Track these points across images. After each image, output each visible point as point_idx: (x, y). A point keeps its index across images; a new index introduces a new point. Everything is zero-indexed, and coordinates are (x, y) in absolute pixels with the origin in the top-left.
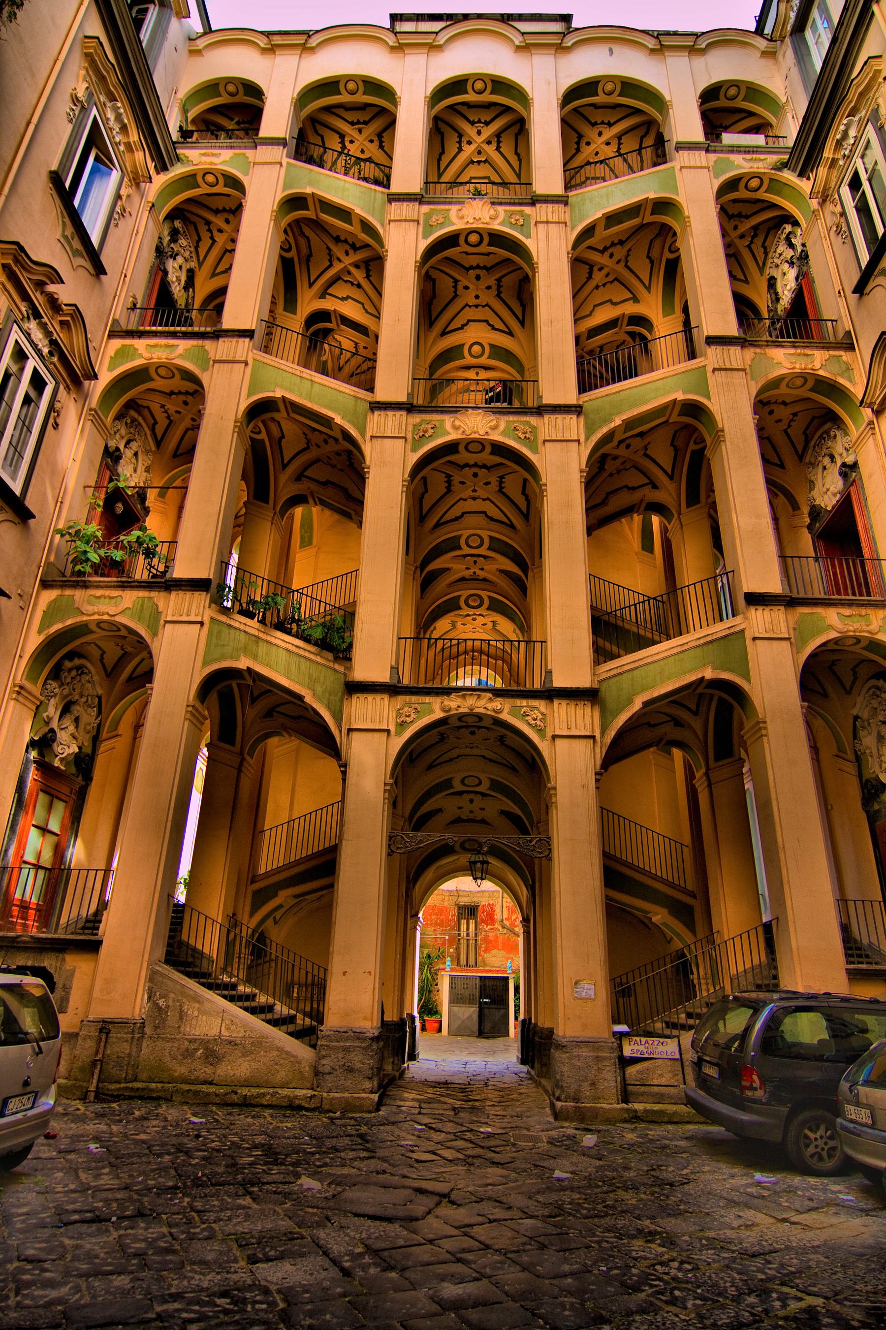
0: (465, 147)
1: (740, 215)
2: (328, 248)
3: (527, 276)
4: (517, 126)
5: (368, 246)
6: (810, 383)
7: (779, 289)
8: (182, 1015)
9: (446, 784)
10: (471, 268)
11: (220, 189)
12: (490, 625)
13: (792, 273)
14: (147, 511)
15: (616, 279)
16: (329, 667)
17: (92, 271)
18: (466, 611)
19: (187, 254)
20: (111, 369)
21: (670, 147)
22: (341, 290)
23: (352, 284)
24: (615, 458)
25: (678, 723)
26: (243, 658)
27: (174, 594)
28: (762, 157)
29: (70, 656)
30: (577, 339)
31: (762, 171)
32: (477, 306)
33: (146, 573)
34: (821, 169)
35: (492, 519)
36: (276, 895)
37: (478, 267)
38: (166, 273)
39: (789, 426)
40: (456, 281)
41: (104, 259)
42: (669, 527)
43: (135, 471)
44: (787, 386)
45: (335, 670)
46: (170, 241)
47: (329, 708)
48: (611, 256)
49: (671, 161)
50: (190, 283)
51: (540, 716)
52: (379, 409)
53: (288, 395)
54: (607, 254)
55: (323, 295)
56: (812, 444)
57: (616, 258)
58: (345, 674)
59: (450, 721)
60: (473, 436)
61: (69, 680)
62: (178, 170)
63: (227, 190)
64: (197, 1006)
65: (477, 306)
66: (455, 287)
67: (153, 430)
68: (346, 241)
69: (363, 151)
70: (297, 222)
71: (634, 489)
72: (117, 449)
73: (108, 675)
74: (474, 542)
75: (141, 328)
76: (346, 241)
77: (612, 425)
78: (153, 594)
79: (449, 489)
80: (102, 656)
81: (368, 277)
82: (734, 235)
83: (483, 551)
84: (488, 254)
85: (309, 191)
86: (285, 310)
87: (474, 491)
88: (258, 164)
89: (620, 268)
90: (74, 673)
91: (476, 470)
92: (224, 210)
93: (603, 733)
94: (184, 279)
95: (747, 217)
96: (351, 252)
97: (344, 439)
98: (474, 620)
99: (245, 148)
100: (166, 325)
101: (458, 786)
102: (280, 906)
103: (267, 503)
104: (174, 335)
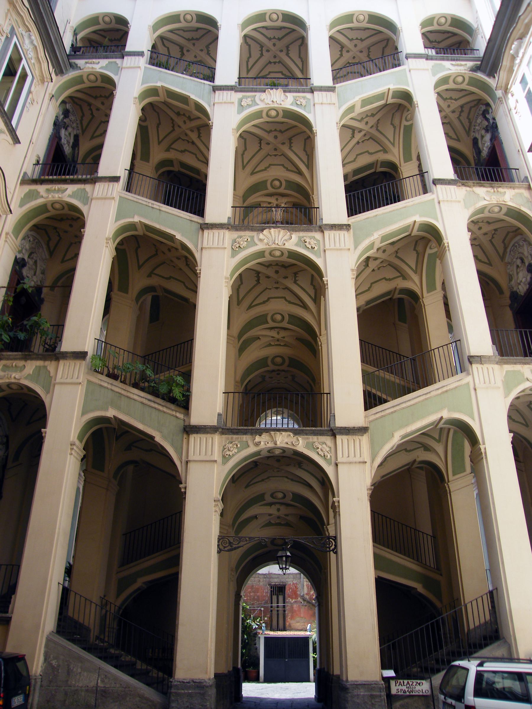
0: (265, 53)
2: (172, 119)
3: (309, 137)
4: (300, 41)
5: (199, 118)
6: (504, 210)
8: (69, 672)
11: (99, 84)
13: (488, 137)
14: (42, 301)
15: (371, 138)
16: (173, 415)
17: (11, 141)
19: (75, 125)
20: (21, 206)
21: (402, 56)
22: (180, 145)
23: (188, 142)
24: (376, 259)
25: (427, 448)
26: (110, 409)
27: (62, 362)
28: (463, 63)
30: (346, 177)
31: (464, 72)
32: (275, 155)
33: (42, 348)
34: (501, 72)
37: (276, 130)
38: (60, 138)
39: (493, 237)
41: (17, 133)
43: (35, 274)
44: (489, 212)
45: (177, 417)
46: (64, 118)
47: (172, 445)
49: (403, 65)
50: (76, 145)
51: (328, 449)
52: (208, 228)
53: (143, 220)
56: (508, 250)
57: (370, 125)
58: (184, 420)
59: (261, 453)
60: (274, 246)
62: (71, 74)
63: (103, 85)
64: (80, 665)
65: (275, 155)
66: (260, 143)
68: (184, 115)
69: (195, 57)
70: (151, 104)
71: (390, 280)
72: (23, 259)
75: (42, 177)
77: (372, 238)
78: (47, 363)
79: (258, 281)
81: (199, 137)
82: (448, 111)
84: (282, 123)
85: (159, 84)
86: (141, 159)
88: (125, 68)
89: (374, 131)
92: (101, 96)
93: (373, 461)
94: (72, 141)
96: (188, 122)
97: (183, 249)
98: (278, 374)
99: (116, 58)
100: (60, 175)
104: (65, 182)
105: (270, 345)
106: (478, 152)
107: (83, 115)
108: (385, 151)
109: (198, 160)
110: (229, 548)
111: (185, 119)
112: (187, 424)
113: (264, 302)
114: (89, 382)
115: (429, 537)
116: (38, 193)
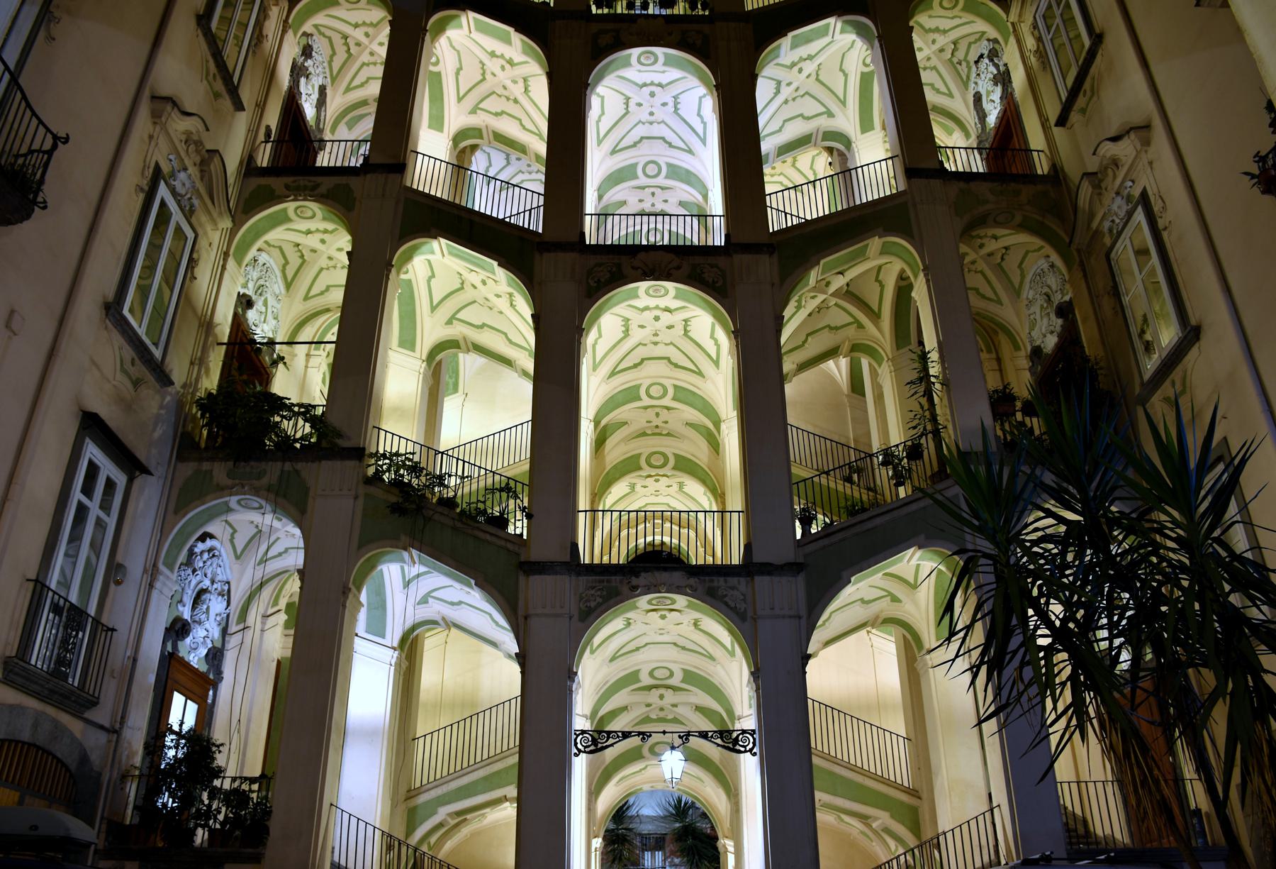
1: (937, 30)
7: (985, 105)
9: (632, 677)
10: (645, 85)
12: (676, 487)
18: (647, 471)
23: (508, 99)
29: (203, 538)
32: (651, 123)
35: (676, 366)
36: (435, 813)
40: (628, 99)
42: (880, 371)
48: (800, 71)
50: (321, 103)
52: (549, 251)
54: (796, 69)
55: (473, 112)
57: (805, 73)
61: (201, 564)
66: (627, 104)
67: (283, 272)
71: (837, 328)
73: (237, 557)
74: (655, 391)
76: (502, 56)
79: (627, 333)
80: (232, 535)
83: (667, 401)
86: (430, 127)
87: (656, 335)
90: (206, 556)
91: (658, 313)
95: (945, 32)
96: (507, 66)
98: (657, 481)
101: (646, 680)
102: (441, 825)
103: (414, 351)
105: (644, 434)
106: (982, 116)
107: (334, 53)
108: (830, 114)
109: (524, 128)
110: (592, 748)
111: (504, 63)
112: (522, 559)
113: (635, 366)
114: (367, 495)
115: (901, 740)
116: (272, 191)
